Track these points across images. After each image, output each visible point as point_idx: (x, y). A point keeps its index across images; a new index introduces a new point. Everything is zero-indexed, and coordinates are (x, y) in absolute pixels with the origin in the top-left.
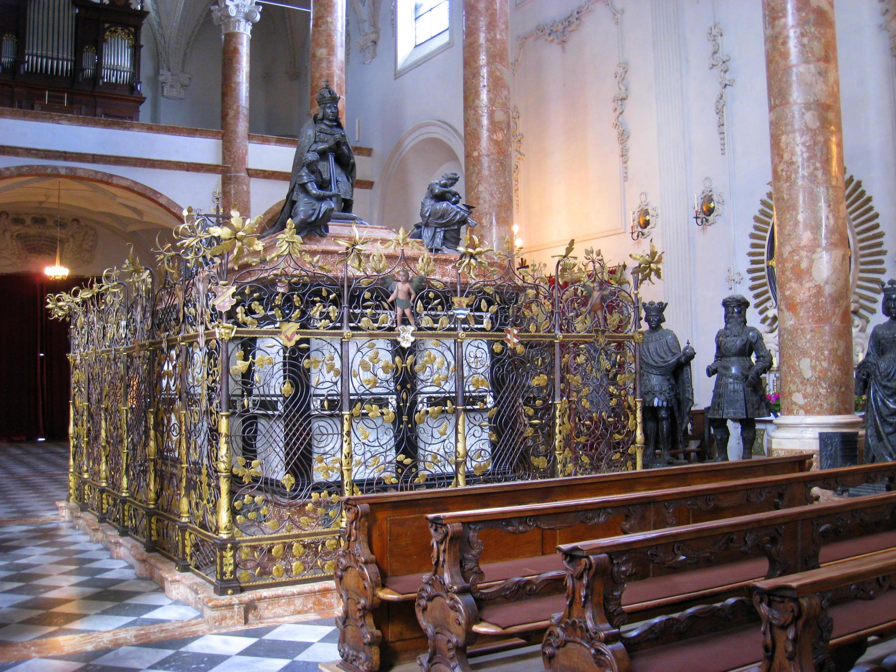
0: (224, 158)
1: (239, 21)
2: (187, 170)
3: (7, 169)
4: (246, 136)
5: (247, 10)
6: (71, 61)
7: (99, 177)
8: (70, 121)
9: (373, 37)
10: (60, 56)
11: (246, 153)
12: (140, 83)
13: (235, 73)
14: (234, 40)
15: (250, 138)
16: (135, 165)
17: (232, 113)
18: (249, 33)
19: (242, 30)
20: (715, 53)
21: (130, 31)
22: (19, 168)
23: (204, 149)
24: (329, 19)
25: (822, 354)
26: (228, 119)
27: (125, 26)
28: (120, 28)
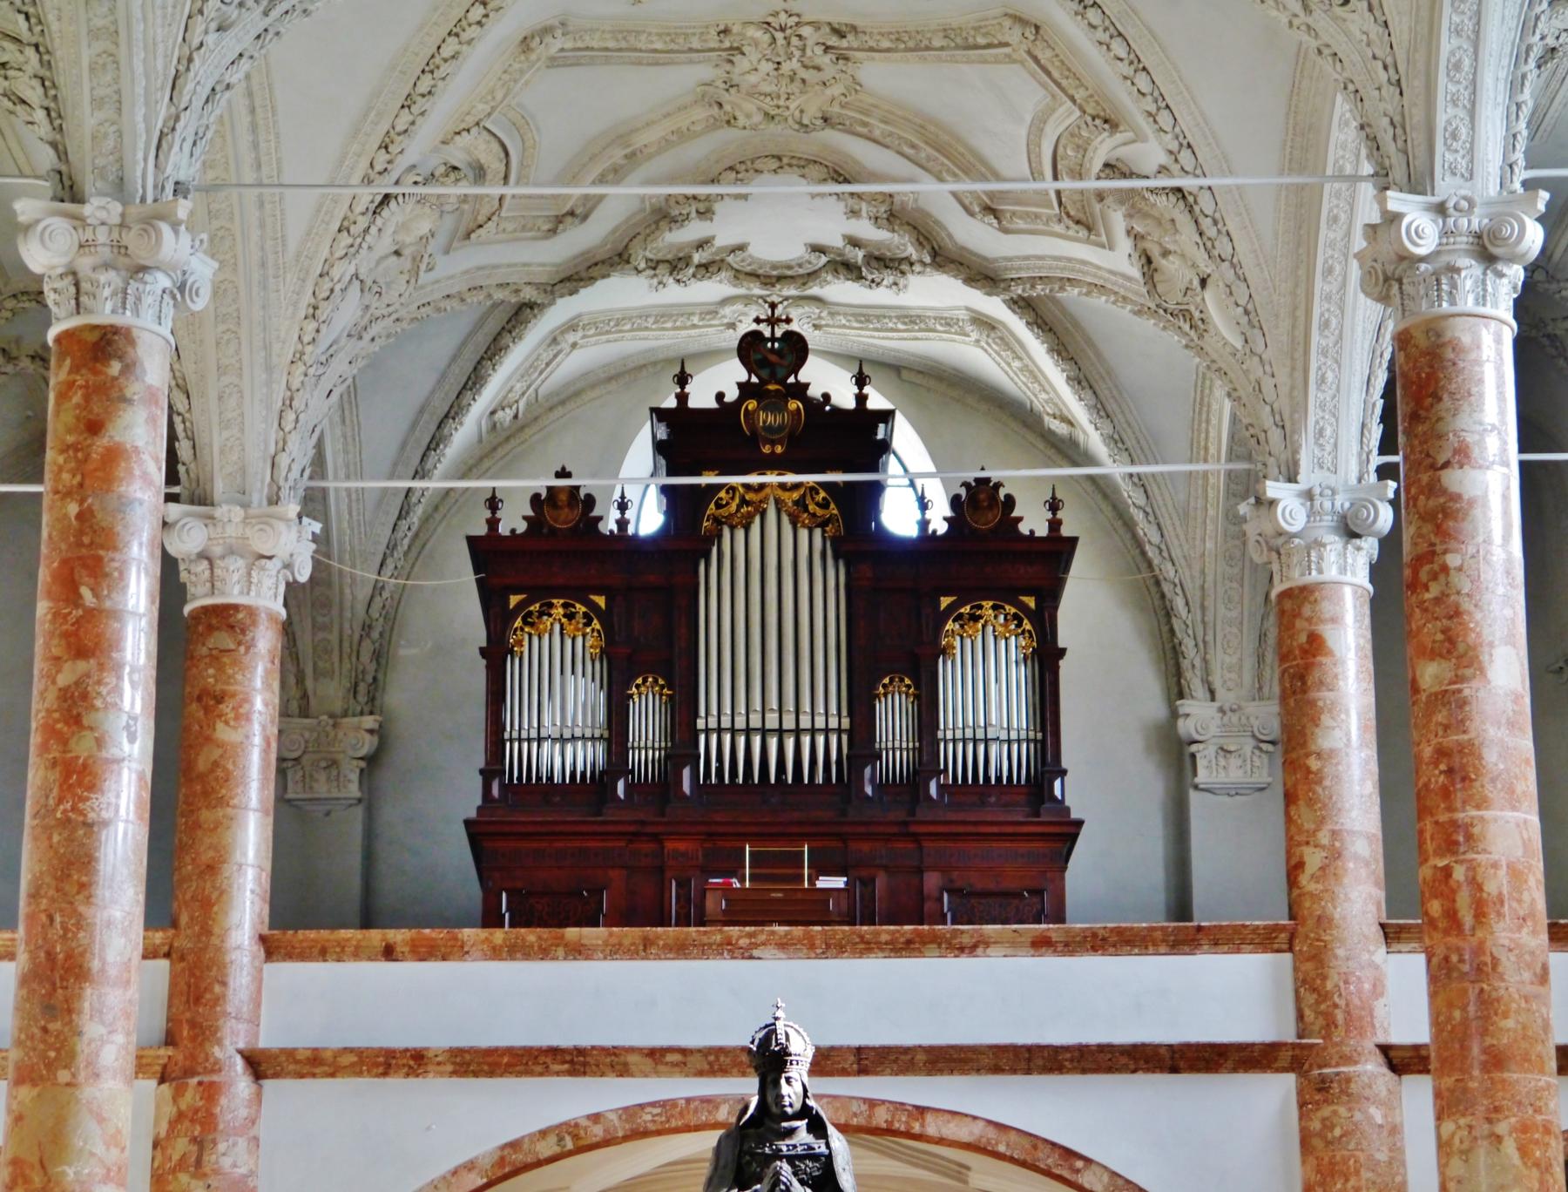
0: (1300, 1016)
1: (1320, 545)
2: (1174, 1070)
3: (596, 1118)
4: (1375, 933)
5: (1342, 502)
6: (839, 731)
7: (881, 1117)
8: (783, 945)
10: (805, 722)
11: (1378, 989)
12: (1063, 773)
13: (1316, 722)
14: (1307, 610)
15: (1392, 935)
16: (997, 1070)
17: (1313, 859)
18: (1362, 577)
19: (1331, 573)
21: (1023, 607)
22: (630, 1112)
23: (1234, 994)
24: (1453, 560)
26: (1304, 879)
27: (1004, 594)
28: (988, 604)
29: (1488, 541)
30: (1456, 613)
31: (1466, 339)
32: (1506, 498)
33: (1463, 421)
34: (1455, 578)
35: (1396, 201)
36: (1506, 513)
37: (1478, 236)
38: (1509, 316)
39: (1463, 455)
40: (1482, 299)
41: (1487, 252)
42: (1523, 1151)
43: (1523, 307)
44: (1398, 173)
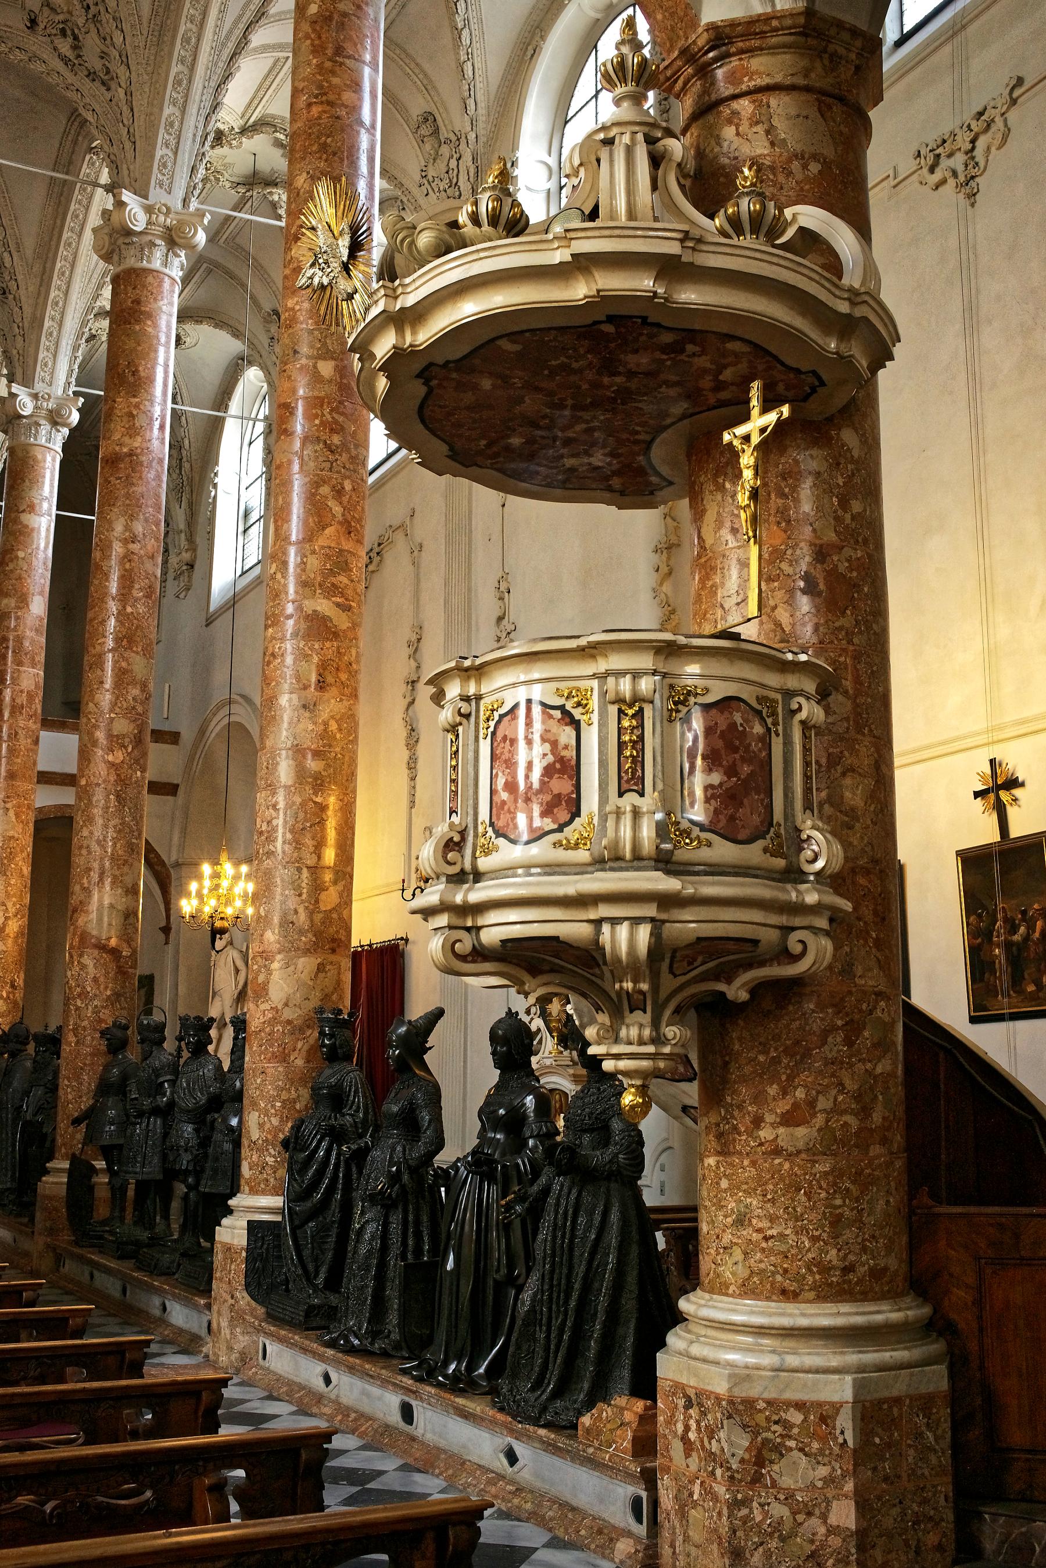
9: (186, 556)
20: (500, 619)
24: (21, 554)
25: (273, 1106)
29: (38, 548)
30: (20, 578)
31: (40, 457)
32: (48, 530)
33: (33, 493)
34: (20, 562)
35: (15, 388)
36: (47, 537)
37: (51, 411)
38: (60, 450)
39: (32, 508)
40: (49, 440)
41: (55, 419)
42: (17, 815)
43: (67, 447)
44: (19, 376)
